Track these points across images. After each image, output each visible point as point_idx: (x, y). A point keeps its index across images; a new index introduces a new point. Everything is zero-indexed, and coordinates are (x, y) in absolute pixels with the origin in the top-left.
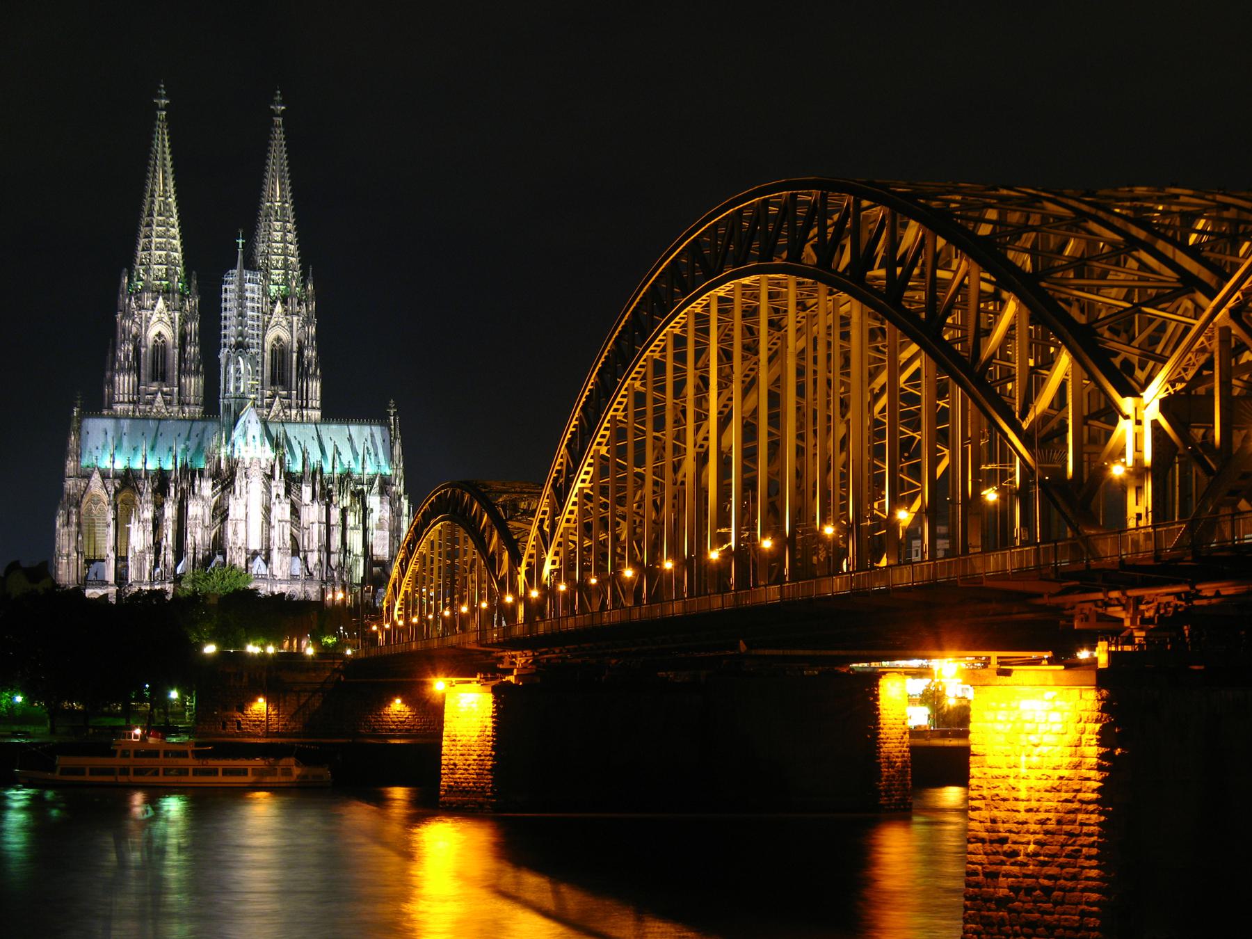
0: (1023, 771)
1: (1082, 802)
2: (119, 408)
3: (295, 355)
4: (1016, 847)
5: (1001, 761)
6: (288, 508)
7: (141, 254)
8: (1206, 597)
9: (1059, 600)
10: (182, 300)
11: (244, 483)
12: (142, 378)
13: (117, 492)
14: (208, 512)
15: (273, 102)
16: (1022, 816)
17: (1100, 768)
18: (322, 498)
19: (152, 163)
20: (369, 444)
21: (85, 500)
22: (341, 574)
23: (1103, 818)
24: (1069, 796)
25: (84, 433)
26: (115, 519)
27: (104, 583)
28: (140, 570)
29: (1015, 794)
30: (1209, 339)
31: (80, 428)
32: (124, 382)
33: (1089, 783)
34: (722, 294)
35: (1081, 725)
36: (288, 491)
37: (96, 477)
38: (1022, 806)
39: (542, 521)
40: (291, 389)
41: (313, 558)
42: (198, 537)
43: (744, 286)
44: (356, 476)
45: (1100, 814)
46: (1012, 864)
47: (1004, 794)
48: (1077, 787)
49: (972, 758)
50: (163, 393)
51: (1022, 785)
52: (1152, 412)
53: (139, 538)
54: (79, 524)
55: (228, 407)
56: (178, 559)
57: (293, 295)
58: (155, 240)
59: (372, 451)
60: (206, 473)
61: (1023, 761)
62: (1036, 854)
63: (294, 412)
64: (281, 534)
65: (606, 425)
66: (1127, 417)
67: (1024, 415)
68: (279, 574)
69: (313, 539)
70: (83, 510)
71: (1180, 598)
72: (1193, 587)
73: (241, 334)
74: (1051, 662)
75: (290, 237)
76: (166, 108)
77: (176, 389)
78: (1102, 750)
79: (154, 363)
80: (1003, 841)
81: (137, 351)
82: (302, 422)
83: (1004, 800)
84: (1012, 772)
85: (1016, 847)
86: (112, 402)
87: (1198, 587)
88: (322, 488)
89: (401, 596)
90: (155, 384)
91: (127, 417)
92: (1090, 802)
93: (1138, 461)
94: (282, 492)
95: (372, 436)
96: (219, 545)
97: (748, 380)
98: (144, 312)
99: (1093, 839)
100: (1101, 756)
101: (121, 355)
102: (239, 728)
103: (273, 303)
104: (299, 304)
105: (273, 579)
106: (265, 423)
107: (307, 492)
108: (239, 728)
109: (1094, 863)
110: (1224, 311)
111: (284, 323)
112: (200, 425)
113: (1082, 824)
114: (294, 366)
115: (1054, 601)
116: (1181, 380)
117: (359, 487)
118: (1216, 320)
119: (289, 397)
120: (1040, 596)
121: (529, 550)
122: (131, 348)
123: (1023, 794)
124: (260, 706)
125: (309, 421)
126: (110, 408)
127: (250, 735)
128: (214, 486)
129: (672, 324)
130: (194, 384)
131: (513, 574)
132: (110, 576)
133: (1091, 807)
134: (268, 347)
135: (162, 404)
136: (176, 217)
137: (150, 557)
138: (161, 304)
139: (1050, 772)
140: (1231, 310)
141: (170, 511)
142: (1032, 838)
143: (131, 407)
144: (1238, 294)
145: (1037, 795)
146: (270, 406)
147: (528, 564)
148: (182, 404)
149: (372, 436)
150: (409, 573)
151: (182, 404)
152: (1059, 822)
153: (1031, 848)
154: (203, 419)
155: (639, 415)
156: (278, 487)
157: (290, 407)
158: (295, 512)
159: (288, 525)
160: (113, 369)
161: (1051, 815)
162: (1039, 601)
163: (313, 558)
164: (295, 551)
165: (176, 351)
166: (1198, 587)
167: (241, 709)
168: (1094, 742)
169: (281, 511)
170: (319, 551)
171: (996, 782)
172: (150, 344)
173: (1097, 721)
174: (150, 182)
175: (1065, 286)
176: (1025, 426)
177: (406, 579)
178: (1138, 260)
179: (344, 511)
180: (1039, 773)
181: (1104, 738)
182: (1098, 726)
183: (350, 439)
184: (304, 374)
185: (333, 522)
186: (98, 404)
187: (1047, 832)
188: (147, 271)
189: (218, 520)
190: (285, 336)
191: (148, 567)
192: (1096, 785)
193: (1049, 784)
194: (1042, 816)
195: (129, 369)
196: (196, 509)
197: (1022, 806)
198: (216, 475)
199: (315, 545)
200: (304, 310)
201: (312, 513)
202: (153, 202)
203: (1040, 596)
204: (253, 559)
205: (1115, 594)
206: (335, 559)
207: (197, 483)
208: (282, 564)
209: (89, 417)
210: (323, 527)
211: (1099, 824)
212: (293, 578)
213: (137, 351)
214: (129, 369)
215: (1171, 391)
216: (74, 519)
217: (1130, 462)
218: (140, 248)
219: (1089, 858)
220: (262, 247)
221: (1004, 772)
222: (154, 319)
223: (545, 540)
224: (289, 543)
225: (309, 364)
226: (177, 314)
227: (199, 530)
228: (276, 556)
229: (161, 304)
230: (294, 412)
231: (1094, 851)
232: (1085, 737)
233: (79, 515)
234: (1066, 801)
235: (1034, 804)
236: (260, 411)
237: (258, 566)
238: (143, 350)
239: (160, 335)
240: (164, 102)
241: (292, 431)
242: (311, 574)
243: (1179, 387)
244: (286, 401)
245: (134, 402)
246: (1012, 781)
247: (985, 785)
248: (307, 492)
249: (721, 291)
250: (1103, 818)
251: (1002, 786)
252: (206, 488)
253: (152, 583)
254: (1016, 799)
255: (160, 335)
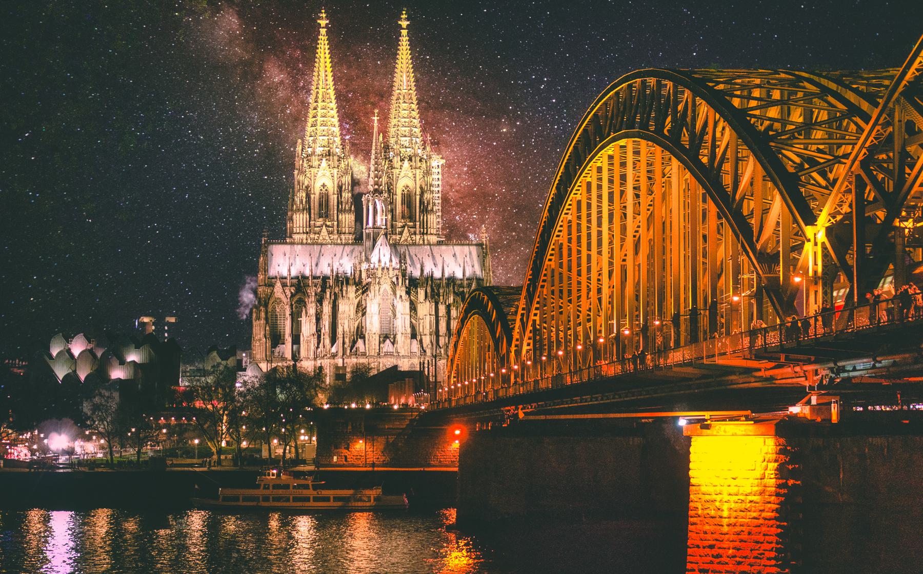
0: (726, 498)
1: (765, 519)
2: (296, 237)
3: (418, 197)
4: (721, 551)
5: (711, 489)
6: (407, 304)
7: (309, 129)
8: (849, 371)
9: (771, 373)
10: (339, 161)
11: (377, 287)
12: (312, 216)
13: (293, 296)
14: (353, 309)
15: (400, 19)
16: (726, 529)
17: (777, 495)
18: (432, 297)
19: (317, 65)
20: (468, 259)
21: (271, 302)
22: (446, 351)
23: (779, 531)
24: (755, 514)
25: (269, 255)
26: (292, 314)
27: (283, 359)
28: (308, 350)
29: (719, 513)
30: (850, 183)
31: (266, 251)
32: (299, 220)
33: (769, 505)
34: (610, 152)
35: (765, 463)
36: (408, 293)
37: (278, 284)
38: (725, 521)
39: (522, 315)
40: (415, 221)
41: (427, 340)
42: (346, 325)
43: (621, 147)
44: (459, 282)
45: (778, 527)
46: (719, 563)
47: (713, 513)
48: (762, 508)
49: (691, 488)
50: (326, 226)
51: (725, 507)
52: (822, 237)
53: (307, 328)
54: (266, 319)
55: (368, 235)
56: (333, 341)
57: (416, 155)
58: (319, 119)
59: (470, 263)
60: (351, 282)
61: (726, 490)
62: (735, 556)
63: (418, 237)
64: (402, 324)
65: (552, 247)
66: (809, 240)
67: (757, 241)
68: (402, 353)
69: (426, 324)
70: (270, 310)
71: (833, 372)
72: (835, 364)
73: (376, 183)
74: (747, 418)
75: (415, 114)
76: (326, 26)
77: (336, 223)
78: (780, 481)
79: (320, 205)
80: (711, 547)
81: (308, 196)
82: (424, 244)
83: (712, 517)
84: (718, 498)
85: (721, 551)
86: (292, 233)
87: (840, 364)
88: (432, 290)
89: (455, 368)
90: (321, 219)
91: (302, 244)
92: (770, 520)
93: (815, 272)
94: (403, 294)
95: (470, 253)
96: (360, 333)
97: (649, 212)
98: (312, 169)
99: (774, 545)
100: (779, 486)
101: (297, 200)
102: (346, 460)
103: (402, 160)
104: (420, 161)
105: (398, 356)
106: (394, 246)
107: (421, 293)
108: (346, 460)
109: (773, 562)
110: (857, 163)
111: (410, 175)
112: (351, 247)
113: (764, 535)
114: (418, 205)
115: (771, 373)
116: (840, 213)
117: (461, 290)
118: (853, 169)
119: (415, 227)
120: (760, 370)
121: (516, 335)
122: (304, 195)
123: (725, 514)
124: (360, 445)
125: (429, 244)
126: (291, 237)
127: (353, 465)
128: (357, 291)
129: (584, 174)
130: (348, 219)
131: (509, 352)
132: (288, 355)
133: (771, 522)
134: (399, 192)
135: (326, 233)
136: (334, 101)
137: (314, 341)
138: (324, 163)
139: (742, 497)
140: (861, 161)
141: (327, 309)
142: (732, 545)
143: (305, 236)
144: (864, 151)
145: (734, 514)
146: (401, 233)
147: (516, 346)
148: (340, 233)
149: (470, 253)
150: (458, 352)
151: (339, 233)
152: (749, 533)
153: (730, 551)
154: (352, 244)
155: (570, 240)
156: (401, 291)
157: (415, 234)
158: (413, 308)
159: (408, 317)
160: (292, 210)
161: (743, 528)
162: (758, 374)
163: (427, 340)
164: (414, 336)
165: (336, 196)
166: (840, 364)
167: (347, 448)
168: (773, 476)
169: (403, 307)
170: (431, 335)
171: (707, 505)
172: (317, 192)
173: (776, 461)
174: (315, 78)
175: (787, 145)
176: (759, 247)
177: (457, 356)
178: (856, 124)
179: (448, 308)
180: (735, 498)
181: (781, 472)
182: (776, 464)
183: (454, 255)
184: (425, 210)
185: (440, 314)
186: (281, 235)
187: (741, 541)
188: (314, 141)
189: (360, 314)
190: (411, 184)
191: (313, 348)
192: (774, 506)
193: (743, 506)
194: (738, 529)
195: (303, 210)
196: (346, 308)
197: (725, 521)
198: (358, 283)
199: (427, 331)
200: (424, 165)
201: (425, 309)
202: (318, 93)
203: (760, 370)
204: (384, 341)
205: (798, 369)
206: (442, 341)
207: (345, 288)
208: (403, 341)
209: (273, 244)
210: (433, 318)
211: (778, 535)
212: (411, 355)
213: (308, 196)
214: (303, 210)
215: (833, 221)
216: (263, 315)
217: (811, 274)
218: (309, 125)
219: (769, 559)
220: (394, 122)
221: (714, 497)
222: (320, 174)
223: (524, 326)
224: (409, 330)
225: (428, 203)
226: (336, 170)
227: (346, 322)
228: (399, 338)
229: (324, 163)
230: (418, 237)
231: (773, 554)
232: (767, 472)
233: (266, 313)
234: (754, 518)
235: (733, 520)
236: (394, 237)
237: (387, 346)
238: (312, 196)
239: (324, 186)
240: (323, 23)
241: (413, 250)
242: (425, 351)
243: (839, 218)
244: (412, 230)
245: (307, 233)
246: (717, 504)
247: (700, 507)
248: (421, 293)
249: (610, 150)
250: (779, 531)
251: (711, 507)
252: (352, 289)
253: (315, 359)
254: (721, 517)
255: (324, 186)
